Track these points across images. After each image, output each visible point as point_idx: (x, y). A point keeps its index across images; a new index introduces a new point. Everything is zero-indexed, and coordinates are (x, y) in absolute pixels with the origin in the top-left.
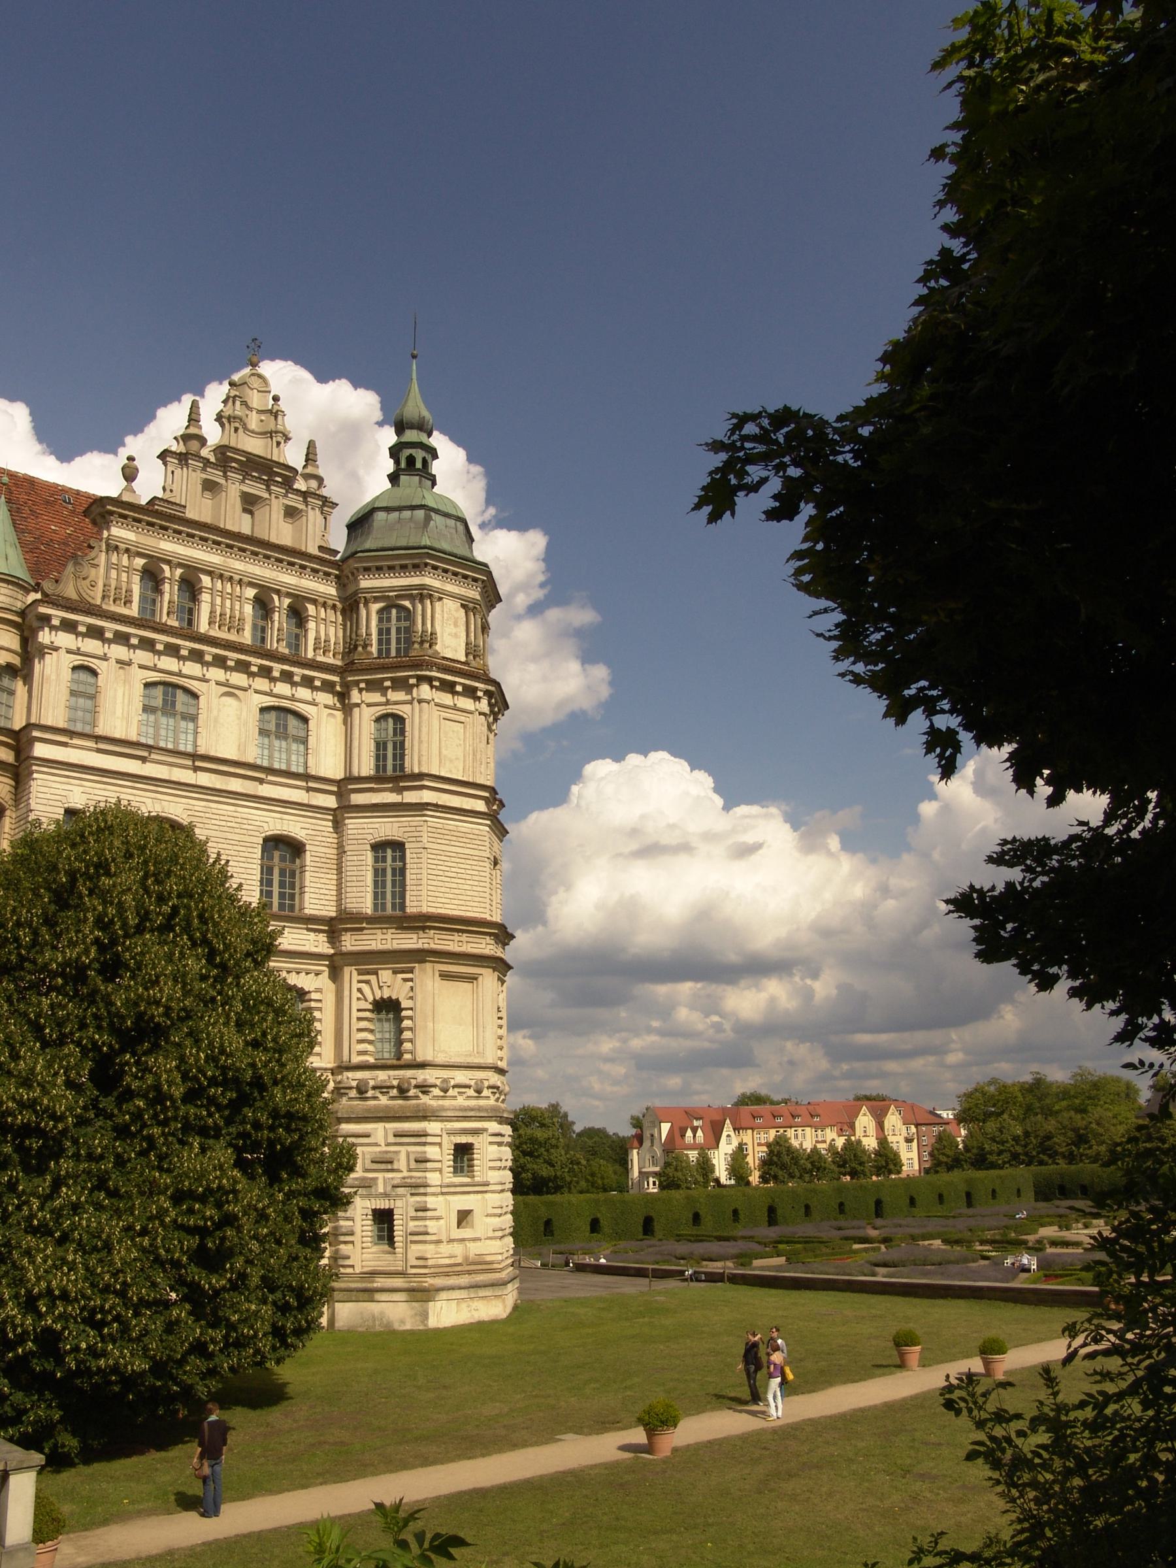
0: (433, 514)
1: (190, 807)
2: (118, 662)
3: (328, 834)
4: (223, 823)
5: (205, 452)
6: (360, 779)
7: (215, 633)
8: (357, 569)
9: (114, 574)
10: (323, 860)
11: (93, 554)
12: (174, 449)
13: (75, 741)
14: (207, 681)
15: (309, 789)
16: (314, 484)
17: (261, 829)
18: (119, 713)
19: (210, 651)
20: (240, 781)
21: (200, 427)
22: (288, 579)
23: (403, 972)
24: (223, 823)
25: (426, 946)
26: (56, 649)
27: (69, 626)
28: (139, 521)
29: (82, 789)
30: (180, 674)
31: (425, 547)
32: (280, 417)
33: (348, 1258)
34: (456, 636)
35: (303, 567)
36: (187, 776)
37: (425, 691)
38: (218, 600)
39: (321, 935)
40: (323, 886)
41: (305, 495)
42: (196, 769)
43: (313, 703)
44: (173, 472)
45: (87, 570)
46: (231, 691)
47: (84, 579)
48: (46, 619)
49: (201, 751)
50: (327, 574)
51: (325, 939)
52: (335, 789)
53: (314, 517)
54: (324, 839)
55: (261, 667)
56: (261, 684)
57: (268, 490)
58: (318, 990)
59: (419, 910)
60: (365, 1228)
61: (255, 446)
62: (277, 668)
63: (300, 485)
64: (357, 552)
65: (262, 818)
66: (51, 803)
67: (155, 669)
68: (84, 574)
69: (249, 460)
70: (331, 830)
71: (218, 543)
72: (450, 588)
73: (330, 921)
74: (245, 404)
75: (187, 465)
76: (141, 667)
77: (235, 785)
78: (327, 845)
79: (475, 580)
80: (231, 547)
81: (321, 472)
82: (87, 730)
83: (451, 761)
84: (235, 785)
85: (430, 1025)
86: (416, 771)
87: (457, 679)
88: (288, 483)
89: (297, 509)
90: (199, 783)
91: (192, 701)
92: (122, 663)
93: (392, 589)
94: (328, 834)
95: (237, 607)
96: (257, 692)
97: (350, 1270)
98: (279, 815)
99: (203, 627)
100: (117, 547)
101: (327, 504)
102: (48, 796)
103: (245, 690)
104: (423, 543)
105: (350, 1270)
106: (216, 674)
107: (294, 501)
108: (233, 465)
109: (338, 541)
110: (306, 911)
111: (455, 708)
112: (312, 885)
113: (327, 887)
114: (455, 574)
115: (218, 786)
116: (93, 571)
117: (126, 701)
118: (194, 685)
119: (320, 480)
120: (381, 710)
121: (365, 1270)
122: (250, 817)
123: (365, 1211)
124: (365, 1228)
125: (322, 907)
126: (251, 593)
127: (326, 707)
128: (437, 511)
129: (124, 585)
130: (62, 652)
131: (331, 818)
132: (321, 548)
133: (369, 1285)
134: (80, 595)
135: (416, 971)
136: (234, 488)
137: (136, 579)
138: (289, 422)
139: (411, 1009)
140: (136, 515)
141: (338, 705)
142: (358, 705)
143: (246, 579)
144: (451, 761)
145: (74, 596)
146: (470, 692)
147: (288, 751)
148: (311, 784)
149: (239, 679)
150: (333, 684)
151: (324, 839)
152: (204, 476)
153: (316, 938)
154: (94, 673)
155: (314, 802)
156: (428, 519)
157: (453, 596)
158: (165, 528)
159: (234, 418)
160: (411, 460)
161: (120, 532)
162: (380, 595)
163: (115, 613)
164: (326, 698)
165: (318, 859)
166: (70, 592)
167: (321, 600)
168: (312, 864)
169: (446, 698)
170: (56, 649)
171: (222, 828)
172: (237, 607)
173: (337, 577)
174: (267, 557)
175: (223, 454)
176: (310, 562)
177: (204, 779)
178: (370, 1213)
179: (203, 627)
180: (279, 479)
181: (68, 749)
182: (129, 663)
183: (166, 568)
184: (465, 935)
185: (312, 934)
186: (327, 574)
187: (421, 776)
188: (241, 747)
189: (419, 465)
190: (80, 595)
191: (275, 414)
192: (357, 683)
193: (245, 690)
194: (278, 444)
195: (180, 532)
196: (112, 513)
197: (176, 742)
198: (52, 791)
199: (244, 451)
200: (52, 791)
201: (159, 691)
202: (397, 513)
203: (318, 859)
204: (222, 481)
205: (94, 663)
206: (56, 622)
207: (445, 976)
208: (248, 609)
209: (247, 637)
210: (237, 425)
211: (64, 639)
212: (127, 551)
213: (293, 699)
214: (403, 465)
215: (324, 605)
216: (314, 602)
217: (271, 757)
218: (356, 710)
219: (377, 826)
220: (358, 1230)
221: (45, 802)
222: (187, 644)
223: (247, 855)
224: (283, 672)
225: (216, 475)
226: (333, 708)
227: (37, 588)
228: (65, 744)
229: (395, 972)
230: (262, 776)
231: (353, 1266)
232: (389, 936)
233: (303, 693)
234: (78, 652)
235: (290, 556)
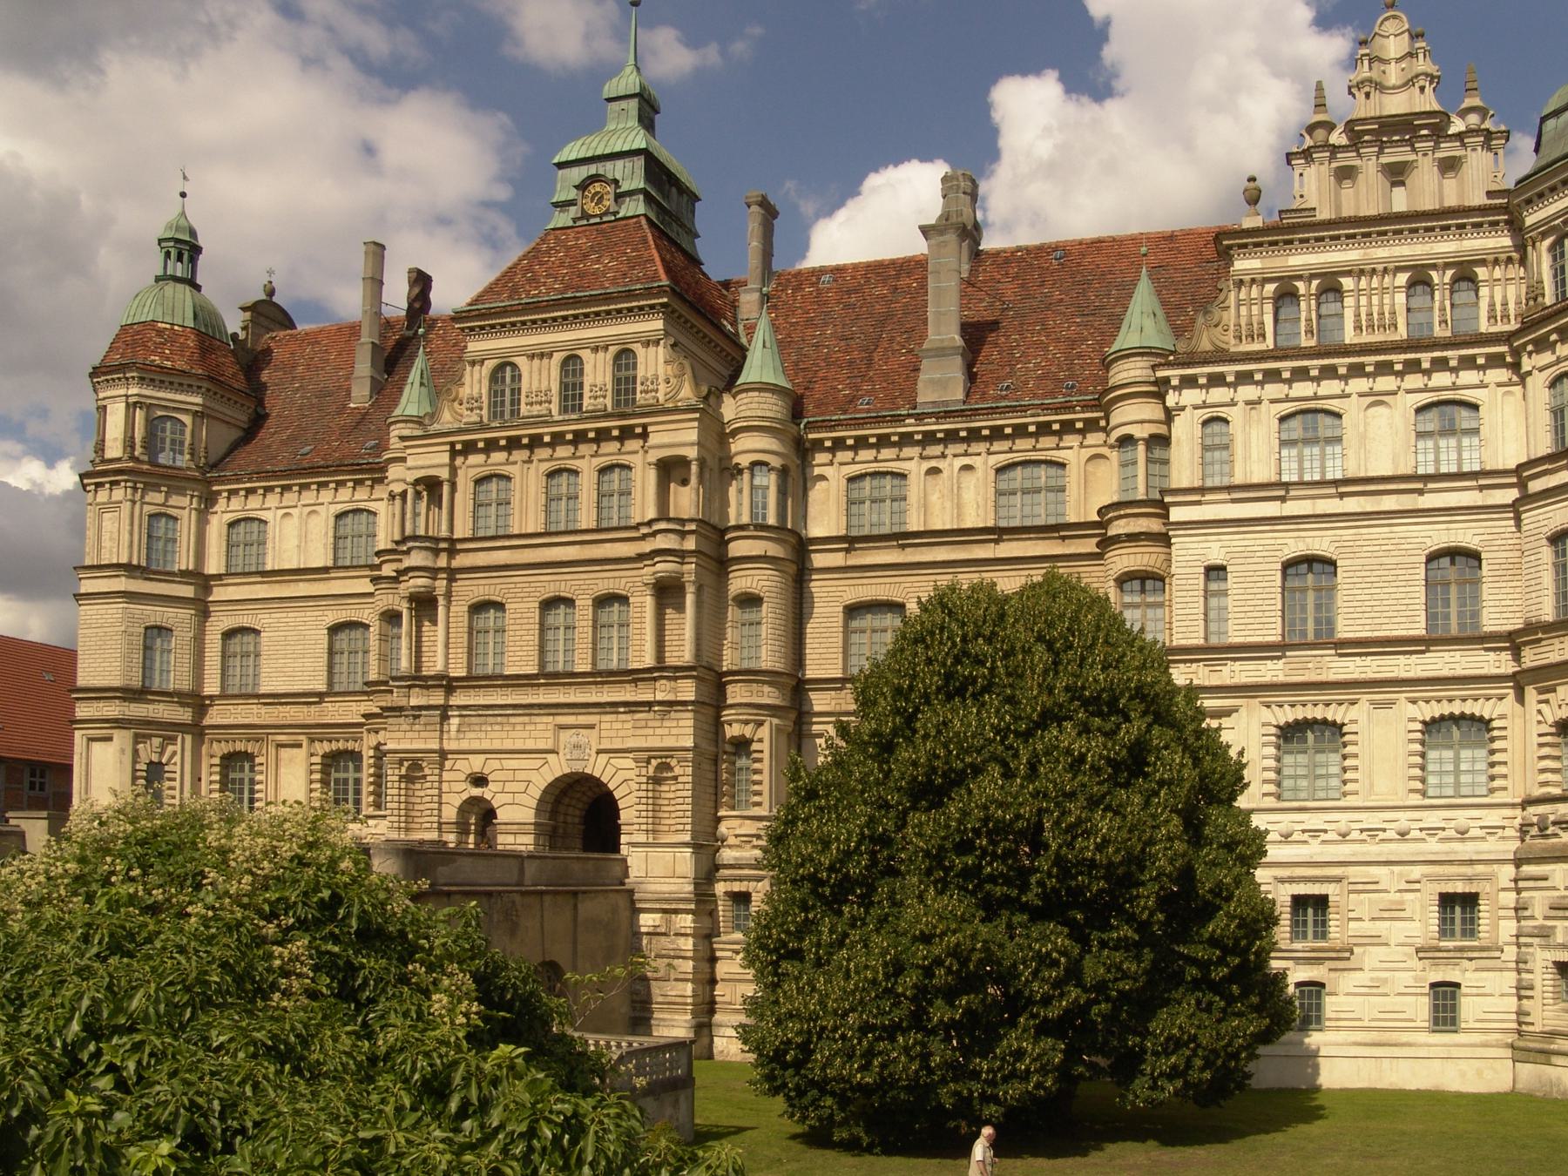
1: (1338, 538)
2: (1248, 403)
3: (1511, 535)
4: (1377, 548)
7: (1366, 338)
9: (1243, 311)
10: (1503, 567)
11: (1222, 297)
13: (1208, 497)
14: (1349, 396)
15: (1481, 488)
17: (1423, 546)
20: (1394, 497)
24: (1377, 548)
26: (1183, 409)
27: (1189, 382)
28: (1260, 245)
29: (1219, 544)
30: (1316, 397)
33: (1529, 1014)
35: (1461, 227)
39: (1504, 653)
40: (1505, 597)
42: (1342, 496)
43: (1482, 385)
44: (1301, 175)
45: (1217, 313)
46: (1377, 399)
47: (1216, 326)
48: (1167, 380)
50: (1496, 223)
51: (1510, 657)
52: (1514, 480)
54: (1504, 542)
55: (1406, 363)
57: (1414, 150)
58: (1502, 717)
60: (1546, 982)
62: (1426, 358)
65: (1423, 534)
66: (1190, 564)
67: (1287, 399)
69: (1382, 126)
70: (1514, 529)
71: (1353, 236)
73: (1510, 636)
75: (1313, 160)
76: (1273, 401)
77: (1389, 503)
78: (1508, 548)
80: (1368, 235)
82: (1226, 481)
84: (1389, 503)
89: (1455, 157)
91: (1337, 422)
92: (1253, 404)
94: (1508, 536)
96: (1408, 392)
97: (1531, 1028)
98: (1444, 526)
99: (1350, 337)
100: (1241, 281)
102: (1188, 558)
103: (1394, 393)
105: (1531, 1028)
108: (1366, 138)
110: (1485, 629)
112: (1491, 597)
113: (1510, 596)
115: (1369, 509)
121: (1547, 1029)
122: (1408, 534)
123: (1545, 964)
124: (1546, 982)
125: (1505, 621)
127: (1499, 385)
129: (1255, 320)
131: (1512, 515)
132: (1490, 194)
133: (1546, 1046)
134: (1213, 344)
136: (1369, 166)
140: (1255, 240)
141: (1515, 378)
143: (1391, 266)
148: (1482, 482)
149: (1385, 383)
150: (1501, 356)
151: (1504, 542)
152: (1334, 165)
153: (1496, 658)
154: (1226, 421)
155: (1490, 502)
158: (1290, 242)
159: (1362, 82)
161: (1244, 264)
163: (1248, 353)
165: (1497, 567)
166: (1205, 345)
167: (1491, 258)
168: (1490, 573)
170: (1183, 409)
171: (1375, 554)
173: (1507, 222)
175: (1352, 130)
176: (1468, 217)
177: (1352, 505)
178: (1551, 965)
180: (1424, 132)
182: (1259, 402)
185: (1492, 654)
186: (1494, 224)
190: (1213, 344)
193: (1394, 393)
195: (1307, 240)
196: (1230, 247)
197: (1323, 473)
198: (1191, 552)
199: (1372, 118)
200: (1191, 552)
201: (1295, 423)
203: (1497, 567)
204: (1357, 162)
205: (1223, 412)
206: (1175, 382)
211: (1191, 396)
212: (1253, 281)
216: (1483, 263)
217: (1437, 461)
220: (1538, 984)
221: (1184, 564)
222: (1315, 362)
223: (1407, 577)
224: (1434, 361)
226: (1510, 383)
230: (1420, 486)
231: (1533, 1024)
233: (1469, 377)
234: (1204, 405)
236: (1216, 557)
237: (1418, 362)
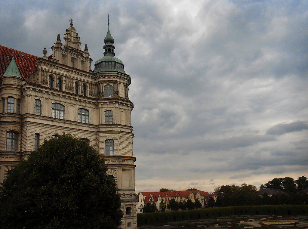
0: (116, 63)
2: (46, 98)
5: (62, 47)
6: (102, 125)
8: (99, 76)
11: (37, 72)
12: (54, 46)
13: (37, 118)
16: (87, 55)
18: (46, 110)
19: (67, 95)
21: (61, 41)
22: (83, 78)
23: (114, 169)
25: (119, 163)
27: (34, 90)
31: (116, 72)
32: (79, 39)
34: (123, 92)
36: (62, 125)
37: (117, 105)
38: (67, 83)
41: (86, 58)
42: (65, 123)
45: (36, 76)
46: (72, 105)
49: (66, 119)
53: (88, 63)
56: (79, 103)
59: (117, 155)
61: (73, 46)
62: (82, 99)
63: (84, 55)
64: (99, 72)
65: (80, 134)
68: (36, 77)
71: (67, 69)
72: (121, 81)
74: (70, 35)
76: (51, 99)
77: (74, 127)
79: (127, 79)
81: (89, 52)
83: (123, 121)
84: (74, 127)
85: (121, 181)
86: (115, 123)
87: (124, 103)
88: (81, 55)
90: (66, 127)
92: (47, 99)
93: (108, 81)
95: (72, 85)
101: (91, 60)
104: (115, 71)
106: (68, 101)
107: (83, 59)
109: (93, 68)
111: (123, 109)
114: (122, 78)
116: (38, 76)
117: (48, 107)
118: (64, 104)
119: (89, 54)
120: (106, 109)
126: (74, 81)
128: (117, 63)
130: (33, 96)
135: (117, 169)
136: (69, 56)
137: (48, 78)
138: (81, 40)
139: (116, 177)
142: (101, 108)
144: (123, 121)
145: (33, 82)
146: (127, 105)
147: (85, 118)
149: (73, 102)
154: (40, 101)
156: (115, 64)
157: (122, 83)
158: (55, 66)
160: (109, 50)
162: (106, 82)
164: (93, 106)
169: (122, 107)
170: (31, 95)
172: (72, 85)
174: (78, 73)
177: (67, 126)
179: (64, 89)
181: (35, 119)
183: (55, 75)
184: (127, 160)
187: (117, 124)
188: (75, 118)
189: (111, 51)
191: (77, 38)
192: (101, 103)
194: (79, 45)
202: (108, 63)
204: (66, 54)
205: (40, 99)
207: (124, 170)
208: (74, 85)
209: (74, 92)
210: (69, 41)
211: (33, 93)
213: (86, 106)
214: (107, 51)
215: (91, 84)
217: (81, 120)
218: (100, 109)
219: (107, 136)
225: (65, 53)
227: (24, 80)
228: (35, 118)
229: (112, 169)
232: (110, 161)
233: (88, 105)
235: (83, 72)
236: (38, 131)
237: (80, 100)
